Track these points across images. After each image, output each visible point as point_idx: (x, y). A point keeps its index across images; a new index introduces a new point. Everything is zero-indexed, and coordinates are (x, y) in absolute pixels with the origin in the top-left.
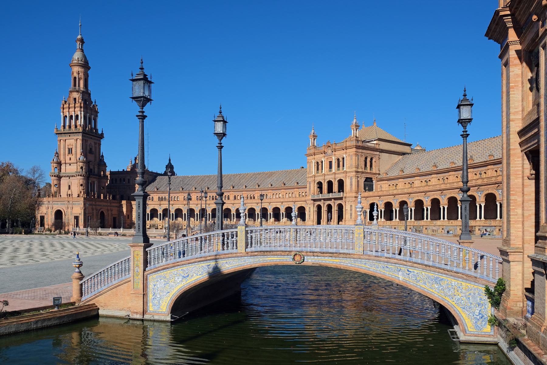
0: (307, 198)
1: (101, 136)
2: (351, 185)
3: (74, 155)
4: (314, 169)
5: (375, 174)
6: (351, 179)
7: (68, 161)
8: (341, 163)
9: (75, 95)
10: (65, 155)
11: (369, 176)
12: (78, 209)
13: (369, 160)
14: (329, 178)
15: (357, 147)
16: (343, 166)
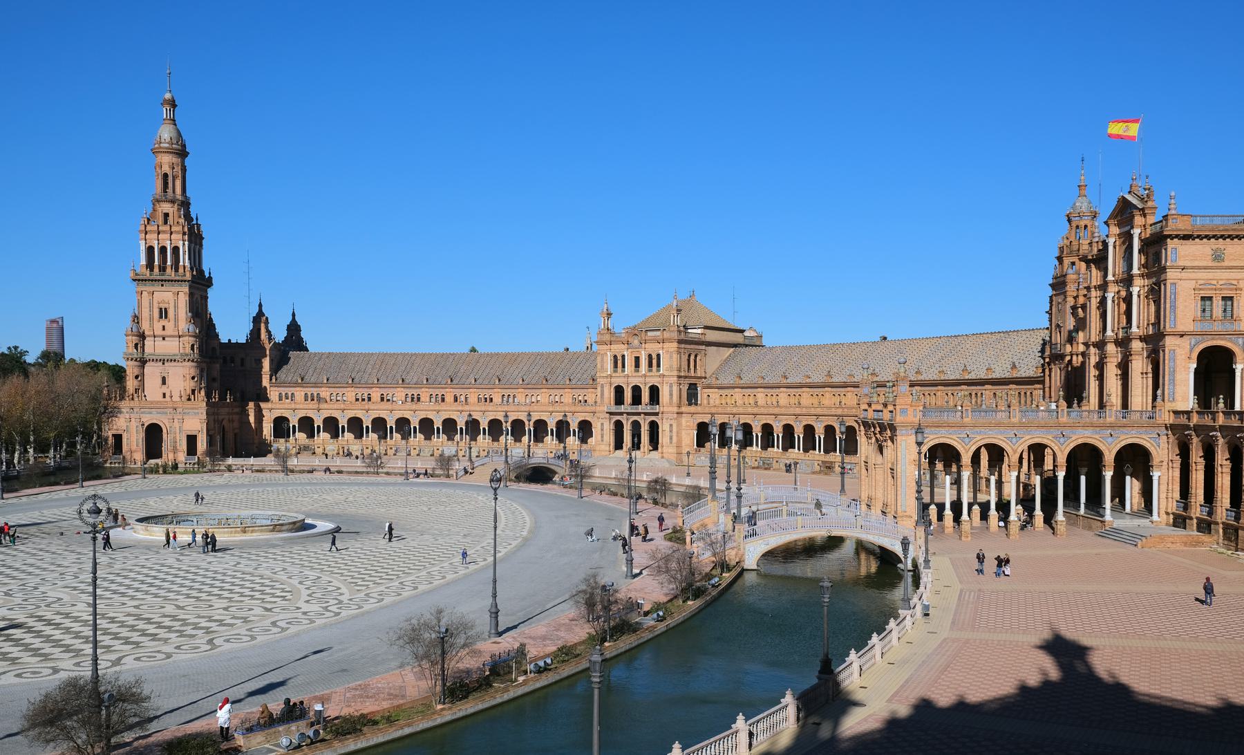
0: (598, 409)
1: (209, 282)
2: (671, 395)
3: (172, 322)
4: (609, 365)
5: (701, 378)
6: (671, 386)
7: (159, 331)
8: (654, 362)
9: (166, 207)
10: (151, 319)
11: (693, 381)
12: (195, 421)
13: (692, 357)
14: (635, 381)
15: (680, 342)
16: (659, 365)
